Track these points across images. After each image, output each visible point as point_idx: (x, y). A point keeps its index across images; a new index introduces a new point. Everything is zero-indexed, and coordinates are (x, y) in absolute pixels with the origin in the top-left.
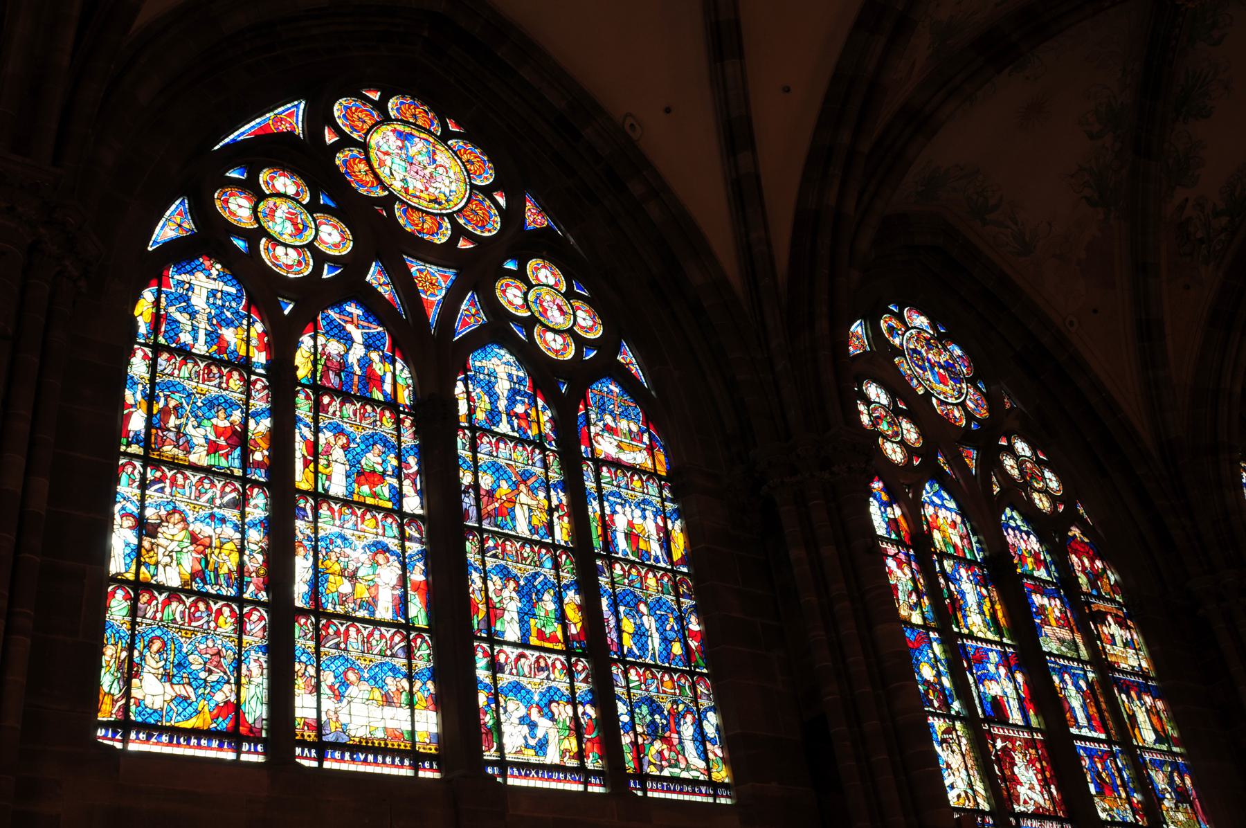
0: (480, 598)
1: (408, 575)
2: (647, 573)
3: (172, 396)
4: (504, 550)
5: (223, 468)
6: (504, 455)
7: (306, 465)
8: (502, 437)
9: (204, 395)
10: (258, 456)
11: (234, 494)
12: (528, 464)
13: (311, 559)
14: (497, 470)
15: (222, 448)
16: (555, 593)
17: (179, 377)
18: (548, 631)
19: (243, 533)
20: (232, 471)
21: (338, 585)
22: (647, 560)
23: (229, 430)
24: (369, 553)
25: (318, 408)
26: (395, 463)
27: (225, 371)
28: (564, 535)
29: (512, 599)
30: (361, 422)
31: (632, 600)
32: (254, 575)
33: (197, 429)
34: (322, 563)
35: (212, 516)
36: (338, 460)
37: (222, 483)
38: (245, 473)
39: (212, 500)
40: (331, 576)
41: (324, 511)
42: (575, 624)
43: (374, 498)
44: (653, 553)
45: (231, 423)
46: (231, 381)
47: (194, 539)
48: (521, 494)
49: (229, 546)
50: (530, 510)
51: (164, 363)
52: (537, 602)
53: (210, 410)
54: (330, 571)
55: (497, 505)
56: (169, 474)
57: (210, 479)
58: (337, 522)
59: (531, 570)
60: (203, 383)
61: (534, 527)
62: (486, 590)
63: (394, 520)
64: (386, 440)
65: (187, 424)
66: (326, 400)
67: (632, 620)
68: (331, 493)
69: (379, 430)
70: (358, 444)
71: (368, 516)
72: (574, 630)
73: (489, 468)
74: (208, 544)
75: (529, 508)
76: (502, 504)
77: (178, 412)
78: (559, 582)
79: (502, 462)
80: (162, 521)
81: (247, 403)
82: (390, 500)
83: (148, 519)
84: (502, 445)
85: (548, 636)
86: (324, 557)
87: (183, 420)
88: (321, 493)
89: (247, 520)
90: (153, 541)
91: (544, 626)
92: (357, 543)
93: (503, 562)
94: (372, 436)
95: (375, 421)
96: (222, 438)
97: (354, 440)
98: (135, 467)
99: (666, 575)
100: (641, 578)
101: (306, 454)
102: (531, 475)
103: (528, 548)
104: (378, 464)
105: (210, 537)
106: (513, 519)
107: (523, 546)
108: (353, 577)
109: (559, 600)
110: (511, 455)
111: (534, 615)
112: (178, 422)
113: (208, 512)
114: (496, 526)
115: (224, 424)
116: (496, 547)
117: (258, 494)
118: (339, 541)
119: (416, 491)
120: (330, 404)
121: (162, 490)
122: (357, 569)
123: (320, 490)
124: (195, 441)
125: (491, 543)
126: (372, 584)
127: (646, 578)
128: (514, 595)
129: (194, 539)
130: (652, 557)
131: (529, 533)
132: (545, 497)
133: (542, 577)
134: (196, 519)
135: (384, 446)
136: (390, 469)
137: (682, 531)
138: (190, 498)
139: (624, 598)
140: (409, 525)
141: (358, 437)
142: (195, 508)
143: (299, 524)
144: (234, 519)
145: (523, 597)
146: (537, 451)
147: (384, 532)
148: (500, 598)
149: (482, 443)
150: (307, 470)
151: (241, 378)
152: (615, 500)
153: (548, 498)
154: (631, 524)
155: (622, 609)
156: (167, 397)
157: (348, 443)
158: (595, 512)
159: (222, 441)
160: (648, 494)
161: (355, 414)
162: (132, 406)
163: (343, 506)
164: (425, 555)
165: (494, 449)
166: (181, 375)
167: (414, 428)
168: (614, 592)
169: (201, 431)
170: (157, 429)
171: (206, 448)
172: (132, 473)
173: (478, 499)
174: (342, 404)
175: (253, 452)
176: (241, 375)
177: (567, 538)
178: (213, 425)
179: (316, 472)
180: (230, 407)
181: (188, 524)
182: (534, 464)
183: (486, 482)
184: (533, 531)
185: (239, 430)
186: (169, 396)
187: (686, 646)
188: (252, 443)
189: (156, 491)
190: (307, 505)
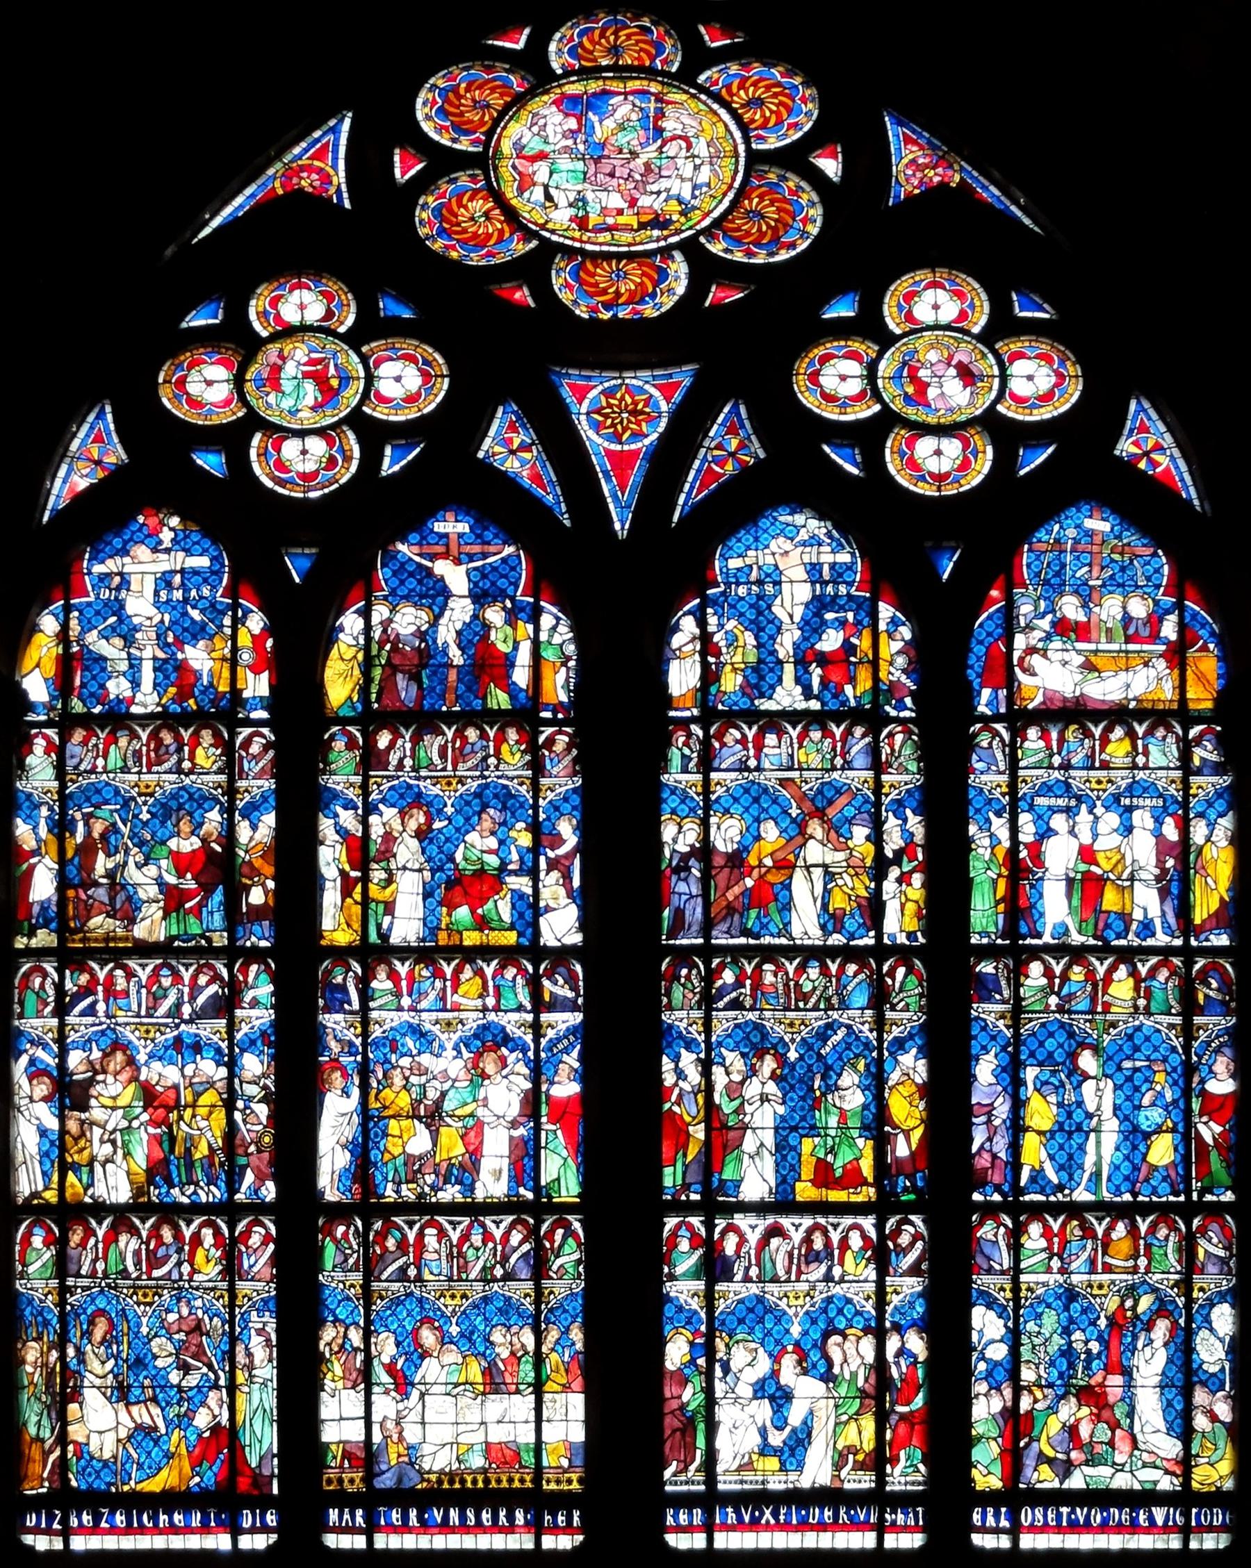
0: (694, 1111)
1: (544, 1088)
2: (1113, 969)
3: (99, 813)
4: (757, 984)
5: (194, 937)
6: (775, 760)
7: (346, 892)
8: (774, 722)
9: (151, 795)
10: (257, 897)
11: (214, 988)
12: (834, 768)
13: (356, 1093)
14: (756, 800)
15: (189, 895)
16: (867, 1066)
17: (105, 771)
18: (838, 1164)
19: (232, 1065)
20: (209, 940)
21: (405, 1138)
22: (1118, 937)
23: (202, 858)
24: (466, 1055)
25: (370, 760)
26: (525, 840)
27: (186, 735)
28: (907, 919)
29: (764, 1098)
30: (455, 769)
31: (1061, 1046)
32: (252, 1149)
33: (145, 869)
34: (377, 1098)
35: (178, 1043)
36: (409, 865)
37: (192, 969)
38: (232, 938)
39: (176, 1011)
40: (393, 1122)
41: (381, 983)
42: (907, 1133)
43: (481, 930)
44: (1138, 915)
45: (203, 840)
46: (200, 752)
47: (148, 1095)
48: (811, 842)
49: (209, 1098)
50: (829, 875)
51: (78, 750)
52: (824, 1094)
53: (163, 823)
54: (391, 1112)
55: (749, 882)
56: (102, 975)
57: (171, 967)
58: (406, 1001)
59: (816, 1020)
60: (149, 772)
61: (833, 916)
62: (709, 1088)
63: (522, 971)
64: (510, 795)
65: (126, 863)
66: (383, 740)
67: (1053, 1099)
68: (395, 939)
69: (492, 775)
70: (449, 819)
71: (468, 972)
72: (902, 1149)
73: (736, 800)
74: (172, 1103)
75: (826, 873)
76: (761, 877)
77: (108, 842)
78: (880, 1039)
79: (769, 778)
80: (96, 1073)
81: (231, 791)
82: (512, 927)
83: (72, 1074)
84: (771, 739)
85: (839, 1173)
86: (379, 1082)
87: (119, 858)
88: (375, 946)
89: (239, 1036)
90: (83, 1116)
91: (832, 1151)
92: (444, 1037)
93: (752, 1016)
94: (478, 795)
95: (485, 759)
96: (189, 876)
97: (440, 811)
98: (45, 975)
99: (1164, 963)
100: (1095, 986)
101: (347, 868)
102: (839, 792)
103: (814, 972)
104: (490, 852)
105: (176, 1087)
106: (788, 906)
107: (802, 969)
108: (433, 1117)
109: (877, 1082)
110: (792, 756)
111: (813, 1127)
112: (110, 865)
113: (170, 1035)
114: (746, 932)
115: (189, 845)
116: (739, 983)
117: (257, 977)
118: (409, 1042)
119: (570, 894)
120: (392, 745)
121: (91, 1011)
122: (444, 1094)
123: (373, 937)
124: (142, 895)
125: (728, 976)
126: (471, 1122)
127: (1108, 980)
128: (771, 1088)
129: (148, 1095)
130: (1134, 926)
131: (819, 933)
132: (868, 838)
133: (841, 1033)
134: (151, 1056)
135: (504, 808)
136: (515, 856)
137: (1232, 842)
138: (139, 1016)
139: (1041, 1044)
140: (550, 974)
141: (449, 803)
142: (148, 1032)
143: (334, 1021)
144: (215, 1038)
145: (792, 1087)
146: (858, 731)
147: (498, 1001)
148: (737, 1102)
149: (723, 745)
150: (349, 900)
151: (218, 741)
152: (1053, 801)
153: (877, 838)
154: (1087, 854)
155: (1030, 1074)
156: (87, 818)
157: (430, 820)
158: (995, 843)
159: (189, 883)
160: (1146, 767)
161: (443, 754)
162: (34, 853)
163: (417, 962)
164: (587, 1035)
165: (752, 752)
166: (110, 767)
167: (575, 752)
168: (1017, 1035)
169: (152, 870)
170: (75, 887)
171: (162, 904)
172: (42, 986)
173: (705, 880)
174: (416, 740)
175: (247, 889)
176: (217, 735)
177: (912, 924)
178: (171, 852)
179: (366, 901)
180: (200, 806)
181: (138, 1069)
182: (848, 766)
183: (726, 835)
184: (830, 927)
185: (219, 849)
186: (91, 815)
187: (1187, 1135)
188: (245, 870)
189: (83, 1014)
190: (347, 978)
